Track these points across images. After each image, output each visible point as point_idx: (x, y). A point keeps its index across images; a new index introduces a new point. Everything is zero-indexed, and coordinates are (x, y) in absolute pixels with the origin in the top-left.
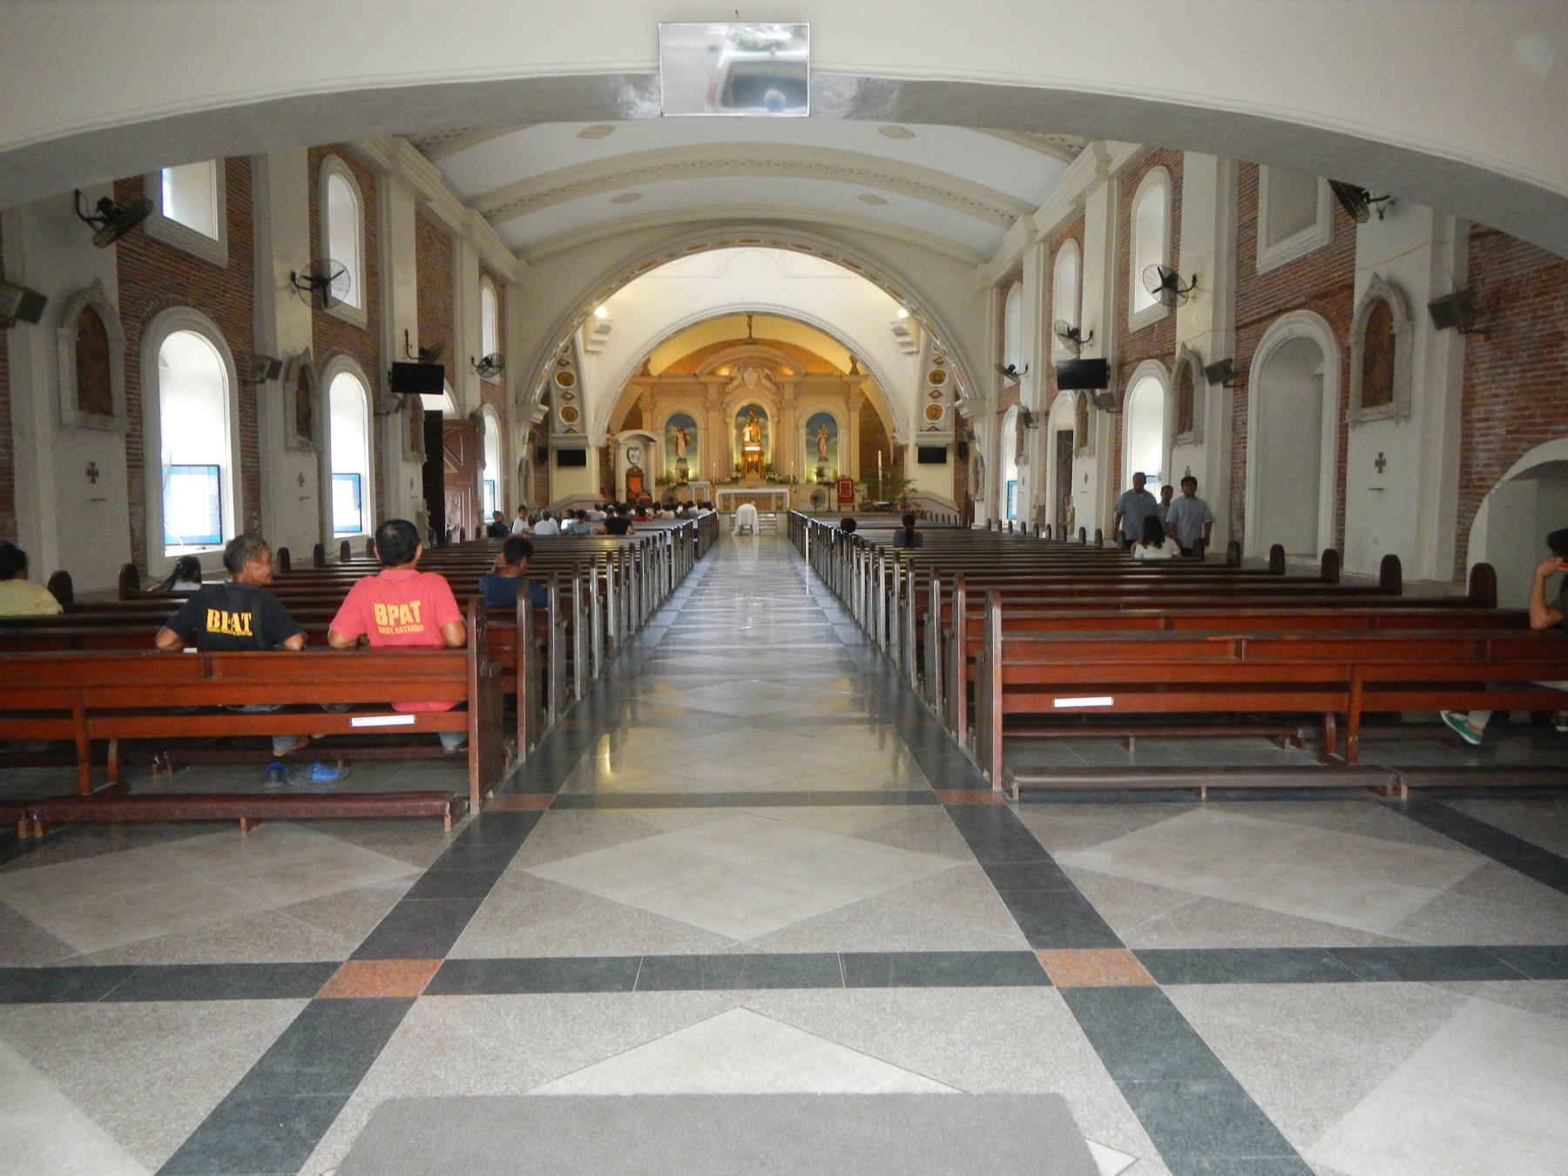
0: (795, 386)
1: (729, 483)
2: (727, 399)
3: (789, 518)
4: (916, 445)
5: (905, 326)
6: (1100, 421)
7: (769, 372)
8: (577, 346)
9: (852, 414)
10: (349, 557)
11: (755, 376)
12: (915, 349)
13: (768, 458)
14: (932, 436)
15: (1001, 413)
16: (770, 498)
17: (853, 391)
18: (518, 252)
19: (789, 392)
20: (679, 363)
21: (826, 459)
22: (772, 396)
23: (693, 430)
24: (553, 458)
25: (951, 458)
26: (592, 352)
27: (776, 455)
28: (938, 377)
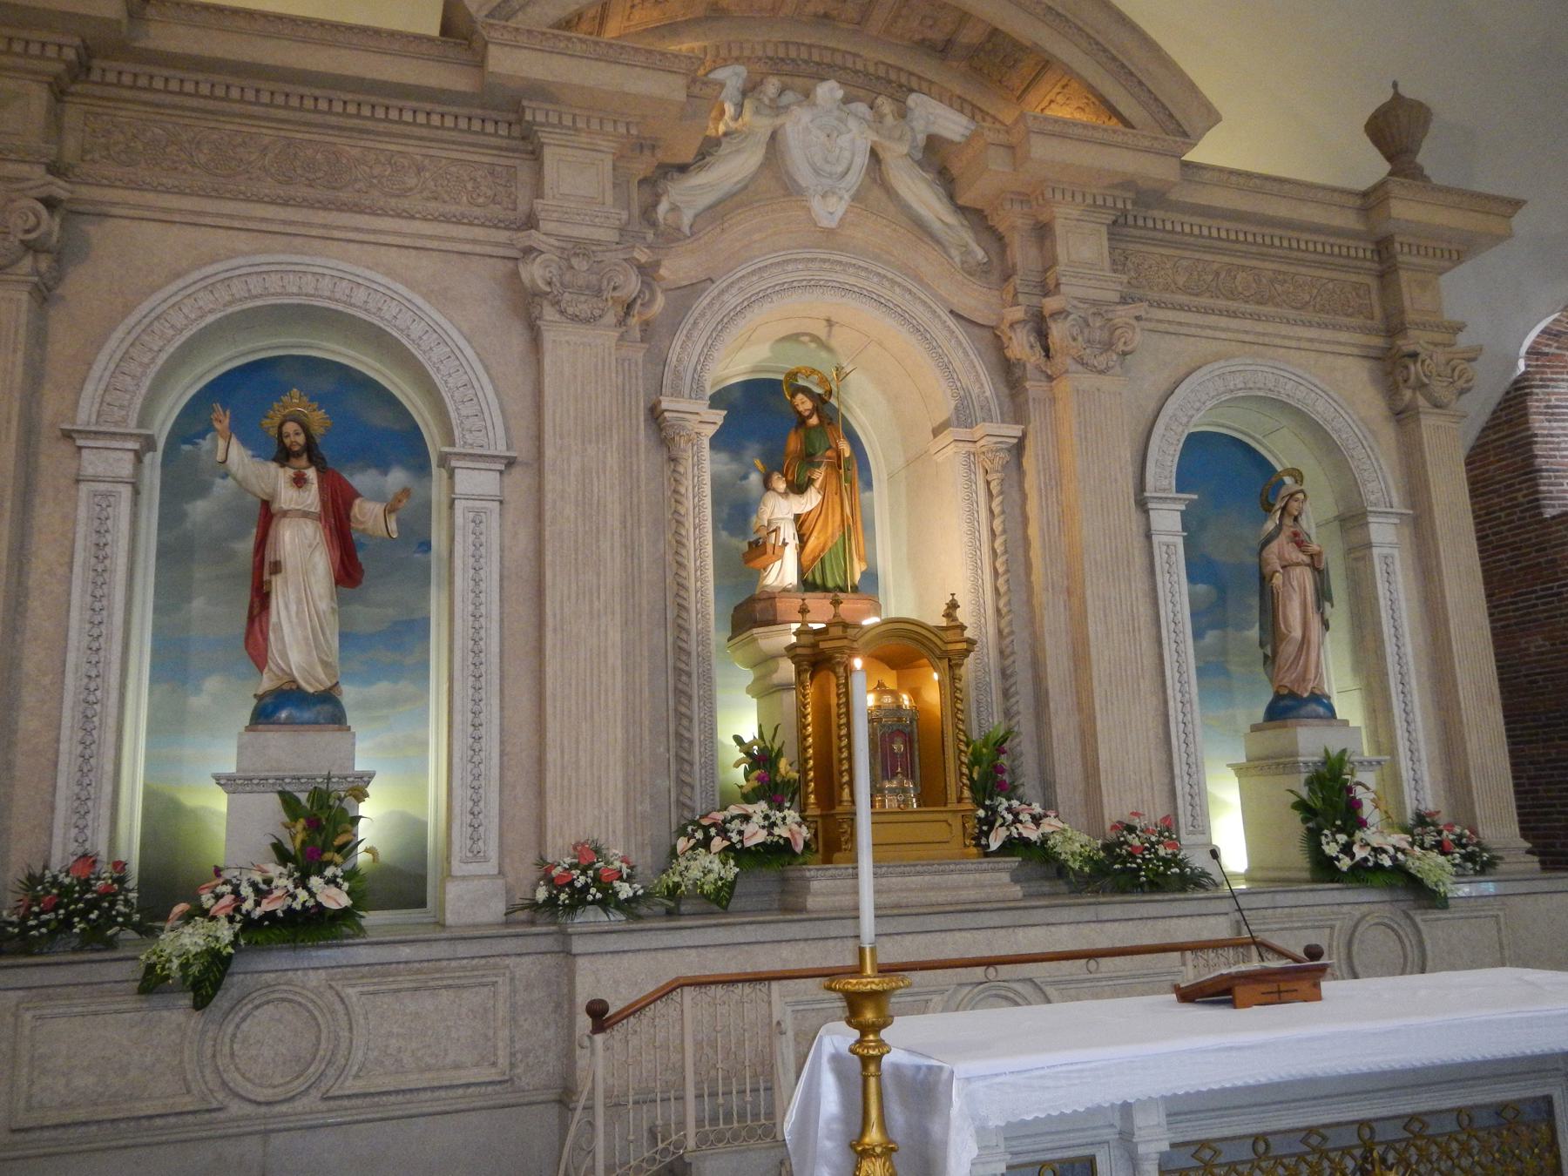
0: (1117, 229)
1: (720, 900)
2: (677, 268)
7: (952, 125)
22: (976, 300)
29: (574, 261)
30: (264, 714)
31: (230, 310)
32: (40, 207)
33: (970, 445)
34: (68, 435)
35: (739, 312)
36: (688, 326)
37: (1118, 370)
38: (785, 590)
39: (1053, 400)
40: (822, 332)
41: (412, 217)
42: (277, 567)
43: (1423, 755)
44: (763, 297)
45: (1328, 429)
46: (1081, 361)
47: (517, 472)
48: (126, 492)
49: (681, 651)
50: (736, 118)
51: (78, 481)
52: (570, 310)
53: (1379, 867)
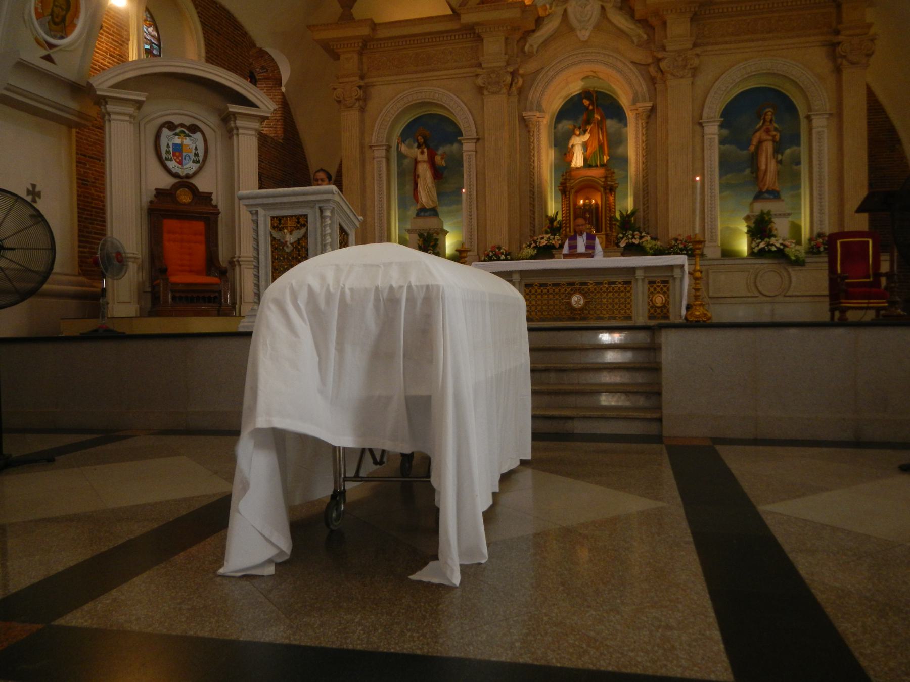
2: (530, 67)
16: (629, 283)
21: (775, 195)
22: (641, 56)
23: (455, 146)
27: (645, 193)
29: (492, 75)
30: (418, 215)
31: (405, 106)
32: (358, 89)
33: (635, 111)
34: (371, 147)
35: (553, 77)
36: (535, 85)
37: (690, 75)
38: (577, 168)
39: (667, 90)
40: (594, 74)
41: (449, 69)
42: (418, 176)
43: (826, 211)
44: (562, 70)
45: (798, 81)
46: (672, 74)
47: (480, 142)
48: (384, 160)
49: (532, 192)
50: (551, 8)
51: (374, 158)
52: (490, 91)
53: (770, 251)
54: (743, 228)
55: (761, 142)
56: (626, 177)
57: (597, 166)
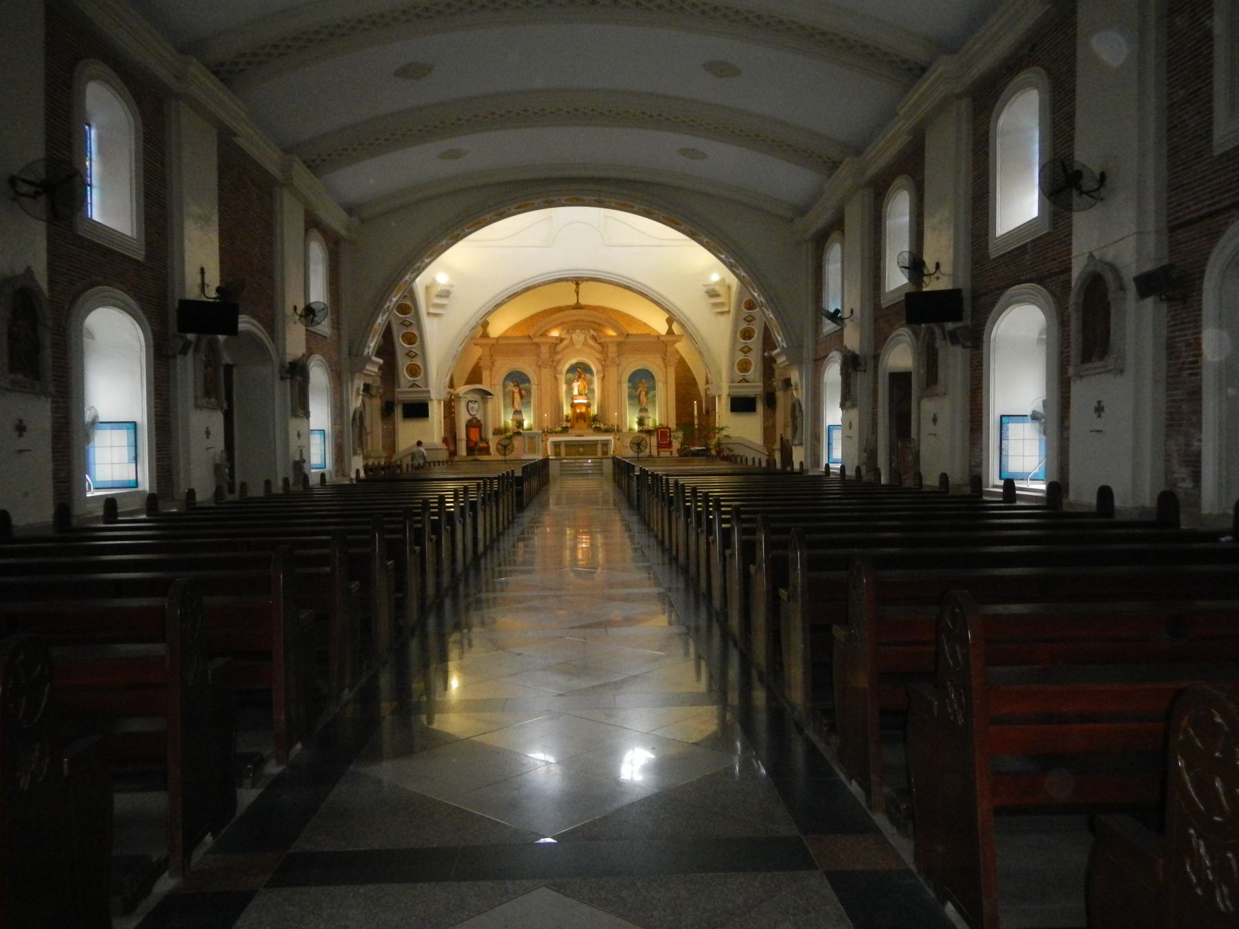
2: (559, 357)
3: (614, 462)
4: (728, 395)
5: (717, 288)
6: (953, 359)
8: (420, 311)
9: (668, 368)
10: (117, 517)
11: (582, 337)
12: (726, 309)
13: (594, 410)
14: (743, 387)
15: (819, 362)
16: (596, 445)
17: (669, 349)
18: (350, 210)
19: (612, 350)
20: (515, 327)
22: (599, 356)
23: (527, 385)
24: (399, 411)
25: (760, 407)
26: (436, 315)
27: (602, 407)
28: (747, 335)
30: (514, 413)
54: (637, 420)
55: (641, 391)
56: (594, 397)
57: (582, 395)
